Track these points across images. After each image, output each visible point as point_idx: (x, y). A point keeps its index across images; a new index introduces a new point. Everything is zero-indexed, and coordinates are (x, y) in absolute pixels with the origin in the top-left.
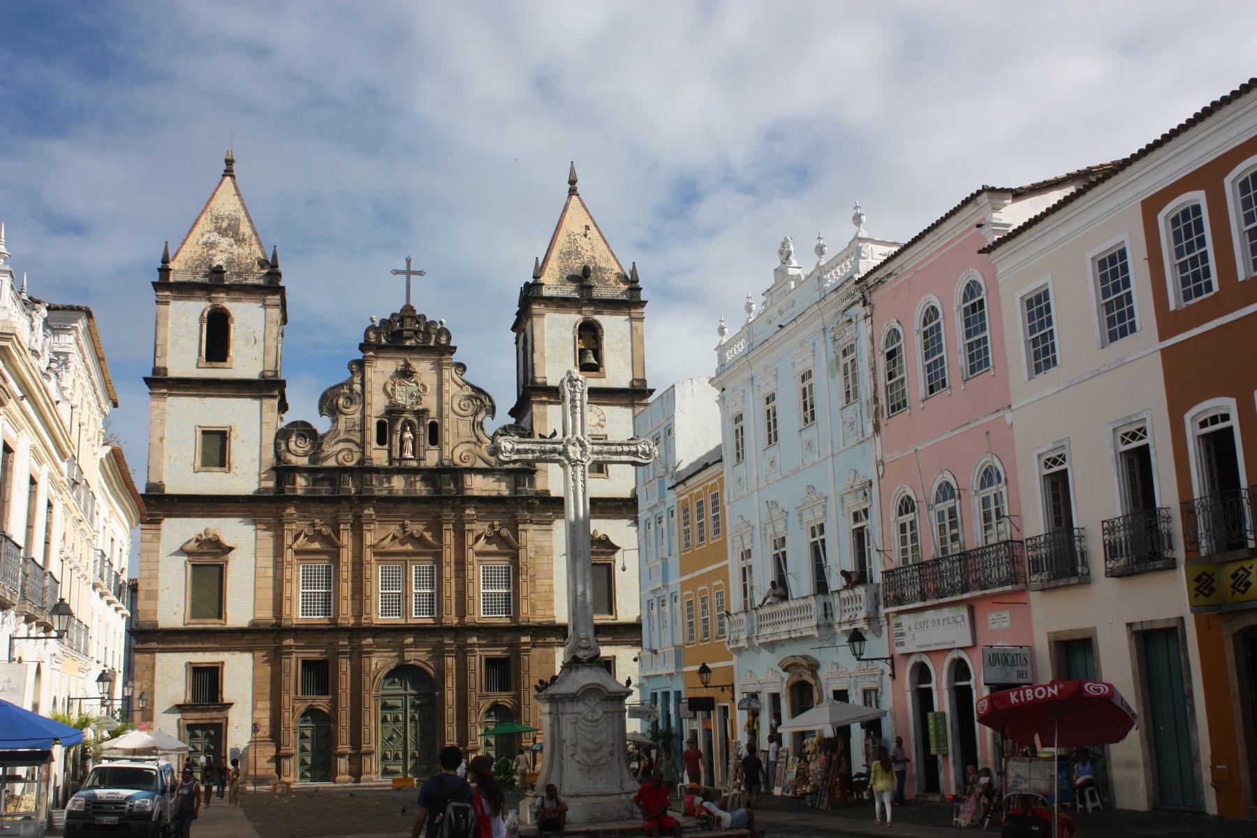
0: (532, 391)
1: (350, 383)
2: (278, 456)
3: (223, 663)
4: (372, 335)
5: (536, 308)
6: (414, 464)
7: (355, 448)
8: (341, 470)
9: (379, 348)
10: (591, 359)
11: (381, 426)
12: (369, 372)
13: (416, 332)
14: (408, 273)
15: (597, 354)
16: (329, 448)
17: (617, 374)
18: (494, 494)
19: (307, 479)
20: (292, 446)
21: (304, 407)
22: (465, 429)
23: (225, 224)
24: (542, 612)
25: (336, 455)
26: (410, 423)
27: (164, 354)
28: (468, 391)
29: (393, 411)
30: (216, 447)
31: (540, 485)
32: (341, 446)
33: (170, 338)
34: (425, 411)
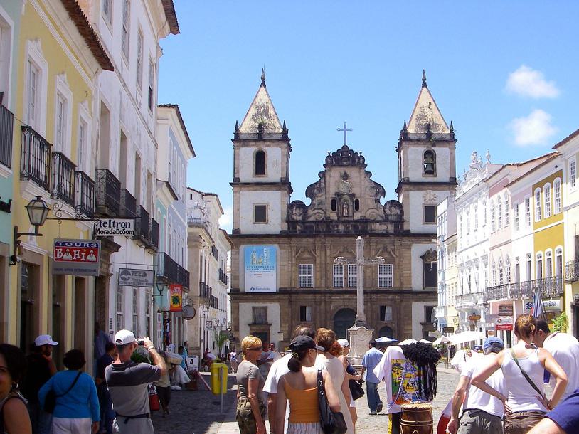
0: (405, 185)
1: (319, 182)
2: (289, 216)
3: (267, 307)
4: (329, 160)
5: (404, 144)
6: (349, 219)
7: (322, 212)
8: (317, 222)
9: (333, 166)
10: (429, 169)
11: (334, 202)
12: (327, 177)
13: (349, 158)
14: (345, 130)
15: (432, 165)
16: (310, 212)
17: (442, 174)
18: (384, 232)
19: (301, 227)
20: (294, 211)
21: (299, 194)
22: (371, 203)
23: (262, 110)
24: (405, 286)
25: (314, 215)
26: (345, 200)
27: (238, 172)
28: (373, 185)
29: (339, 195)
30: (261, 213)
31: (405, 227)
32: (316, 211)
33: (240, 165)
34: (353, 195)
